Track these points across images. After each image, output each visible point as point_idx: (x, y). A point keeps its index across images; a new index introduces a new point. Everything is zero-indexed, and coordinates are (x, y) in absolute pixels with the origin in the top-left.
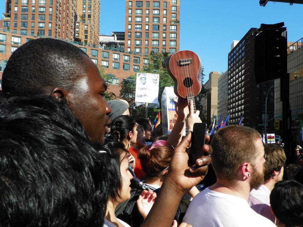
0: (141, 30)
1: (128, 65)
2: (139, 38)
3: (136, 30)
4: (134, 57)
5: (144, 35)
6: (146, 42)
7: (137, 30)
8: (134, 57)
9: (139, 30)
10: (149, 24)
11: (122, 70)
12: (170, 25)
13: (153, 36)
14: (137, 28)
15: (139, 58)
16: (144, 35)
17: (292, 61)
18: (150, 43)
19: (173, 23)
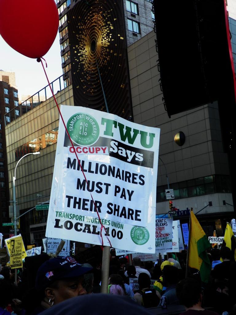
17: (33, 122)
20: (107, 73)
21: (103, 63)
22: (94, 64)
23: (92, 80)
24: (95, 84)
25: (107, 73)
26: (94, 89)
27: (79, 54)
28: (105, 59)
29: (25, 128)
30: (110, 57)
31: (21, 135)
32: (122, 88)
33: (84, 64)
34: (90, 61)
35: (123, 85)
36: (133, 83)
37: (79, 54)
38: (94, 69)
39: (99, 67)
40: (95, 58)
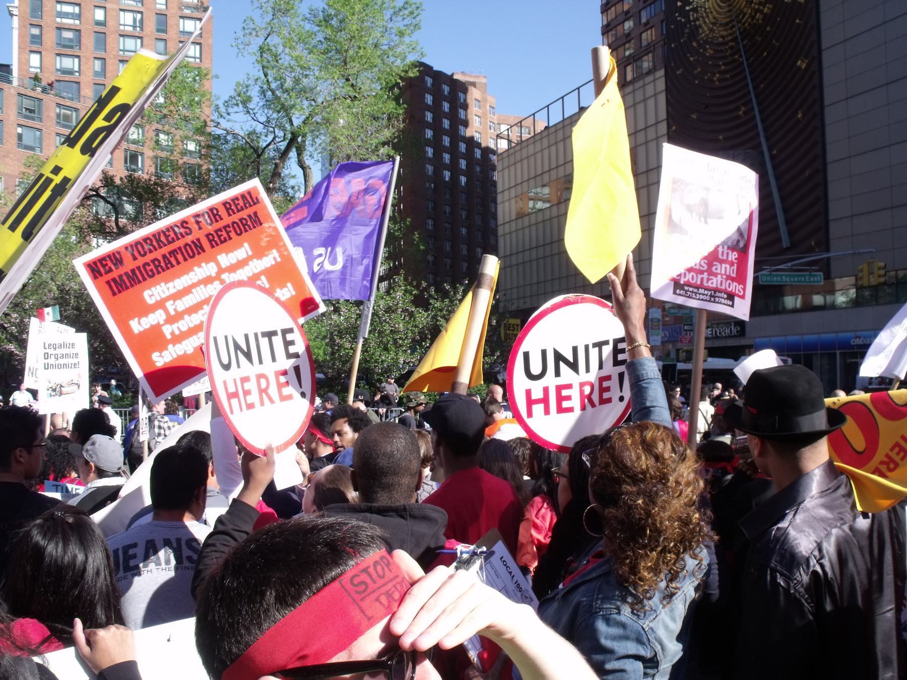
0: (77, 22)
1: (38, 133)
2: (72, 47)
3: (58, 20)
4: (59, 105)
5: (88, 41)
6: (98, 65)
7: (65, 21)
8: (59, 105)
9: (71, 21)
10: (108, 5)
11: (15, 147)
12: (181, 17)
13: (122, 48)
14: (66, 15)
15: (76, 110)
16: (88, 41)
18: (109, 68)
19: (187, 12)
20: (760, 39)
21: (752, 20)
22: (727, 24)
23: (722, 55)
24: (724, 64)
25: (760, 39)
26: (719, 73)
27: (687, 8)
28: (757, 11)
29: (515, 169)
30: (771, 6)
31: (513, 178)
32: (799, 68)
33: (700, 26)
34: (715, 18)
35: (802, 61)
36: (827, 58)
37: (687, 8)
38: (724, 33)
39: (739, 29)
40: (730, 11)
